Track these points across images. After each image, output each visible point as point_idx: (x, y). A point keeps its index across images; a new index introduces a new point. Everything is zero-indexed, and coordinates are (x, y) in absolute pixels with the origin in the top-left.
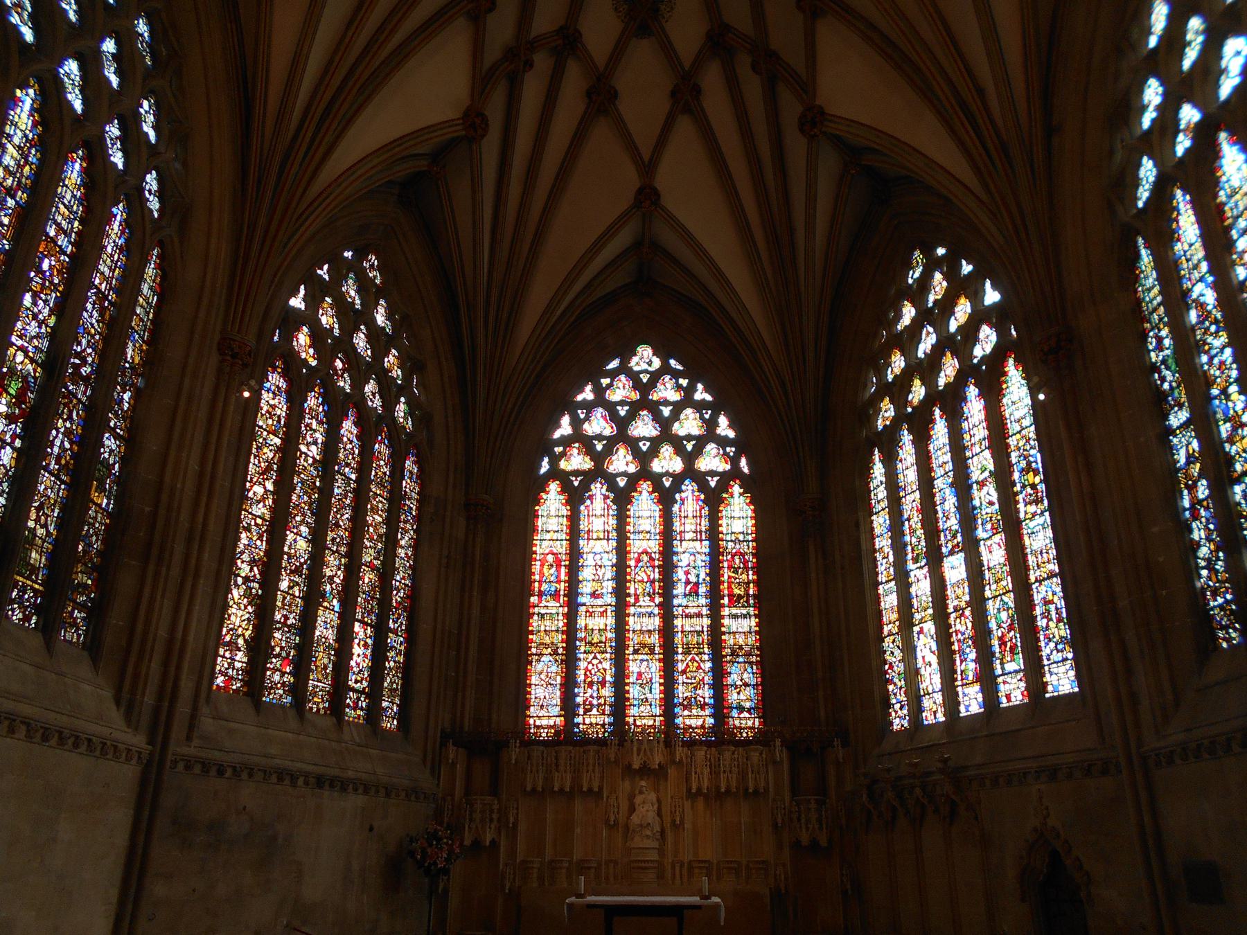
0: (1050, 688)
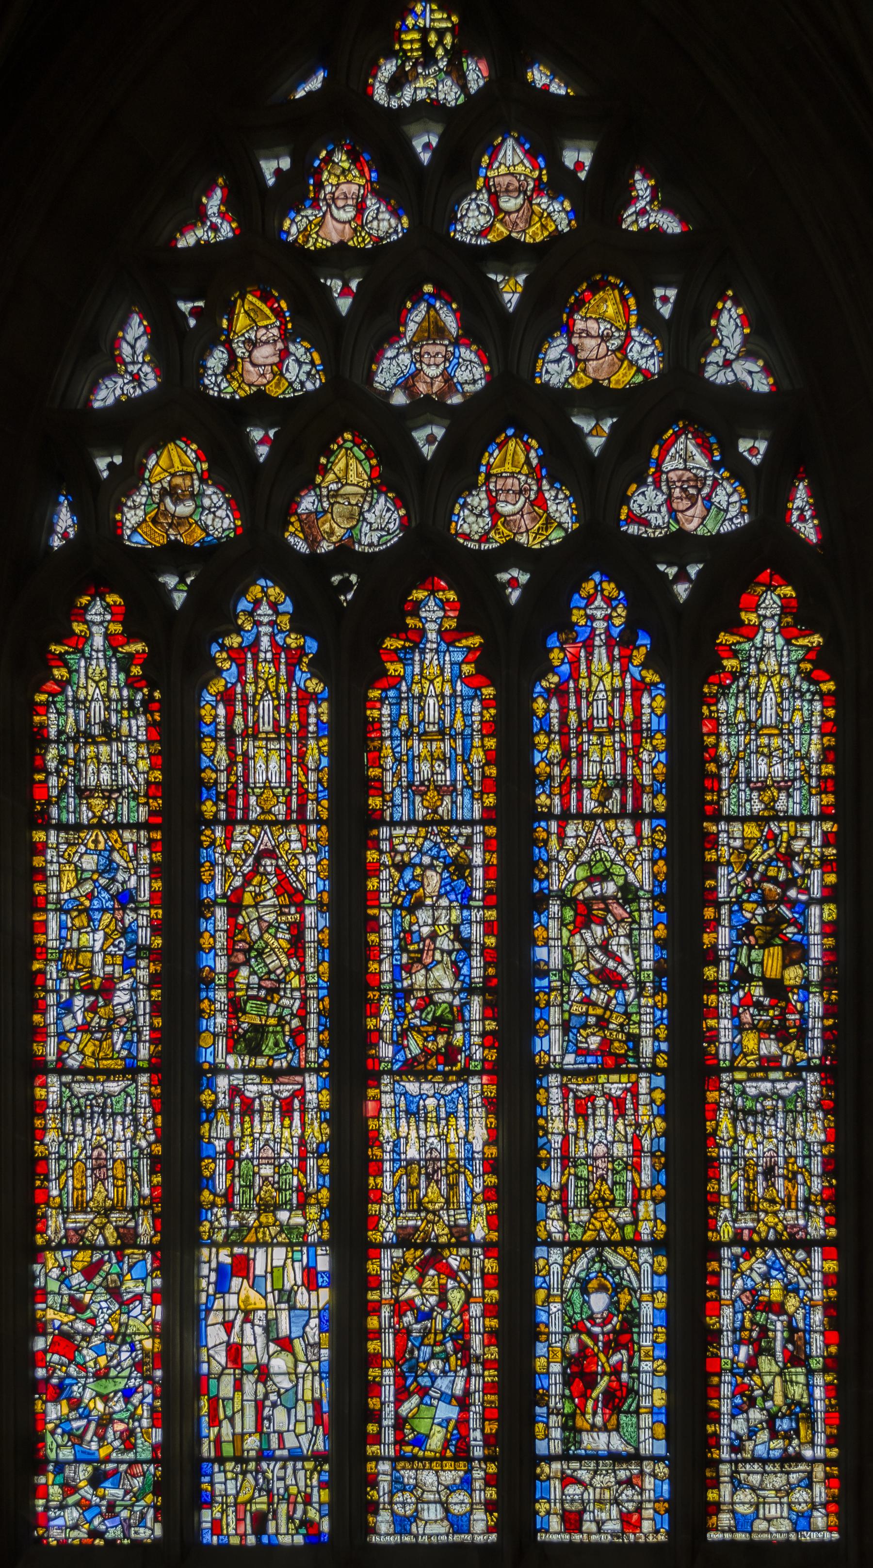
0: (725, 1519)
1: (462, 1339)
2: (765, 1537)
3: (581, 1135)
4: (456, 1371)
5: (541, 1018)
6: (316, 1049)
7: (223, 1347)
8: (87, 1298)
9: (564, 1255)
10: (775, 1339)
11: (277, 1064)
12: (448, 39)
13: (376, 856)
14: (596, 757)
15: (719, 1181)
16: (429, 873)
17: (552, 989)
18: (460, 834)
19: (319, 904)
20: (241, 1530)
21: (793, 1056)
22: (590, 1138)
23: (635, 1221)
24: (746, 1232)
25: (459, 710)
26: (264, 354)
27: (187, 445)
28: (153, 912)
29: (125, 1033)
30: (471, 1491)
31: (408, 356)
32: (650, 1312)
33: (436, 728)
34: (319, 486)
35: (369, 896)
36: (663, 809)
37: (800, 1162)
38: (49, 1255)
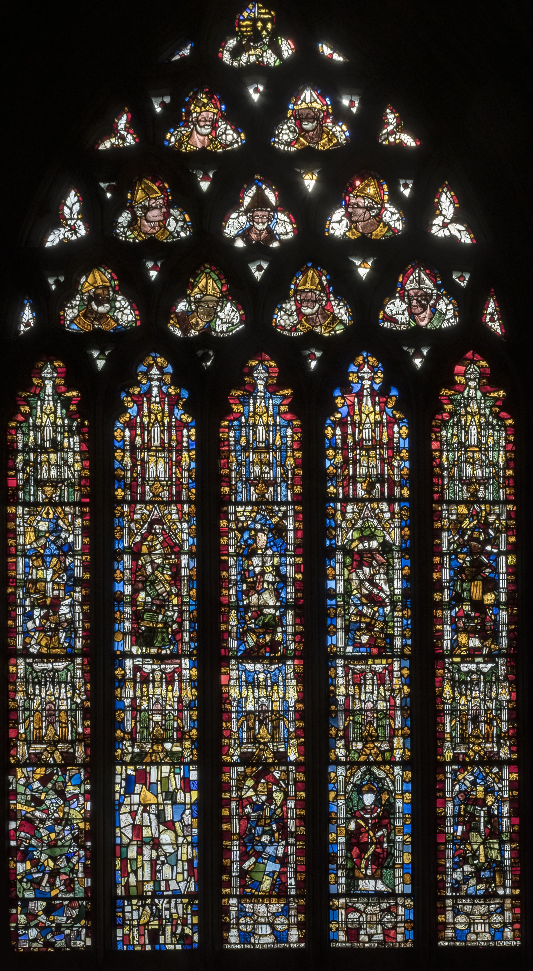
1: (282, 822)
2: (475, 944)
3: (357, 696)
4: (278, 842)
5: (331, 624)
6: (188, 643)
7: (130, 827)
8: (43, 797)
9: (347, 770)
10: (479, 821)
11: (164, 652)
12: (269, 26)
13: (226, 524)
14: (364, 463)
15: (444, 724)
16: (260, 534)
17: (338, 606)
18: (280, 510)
19: (190, 554)
20: (142, 942)
21: (490, 648)
22: (363, 698)
23: (392, 749)
24: (461, 756)
25: (278, 434)
26: (155, 215)
27: (106, 270)
28: (84, 557)
29: (66, 632)
30: (288, 916)
31: (245, 217)
32: (401, 805)
33: (264, 445)
34: (189, 296)
35: (222, 549)
36: (407, 496)
37: (494, 713)
38: (18, 770)
